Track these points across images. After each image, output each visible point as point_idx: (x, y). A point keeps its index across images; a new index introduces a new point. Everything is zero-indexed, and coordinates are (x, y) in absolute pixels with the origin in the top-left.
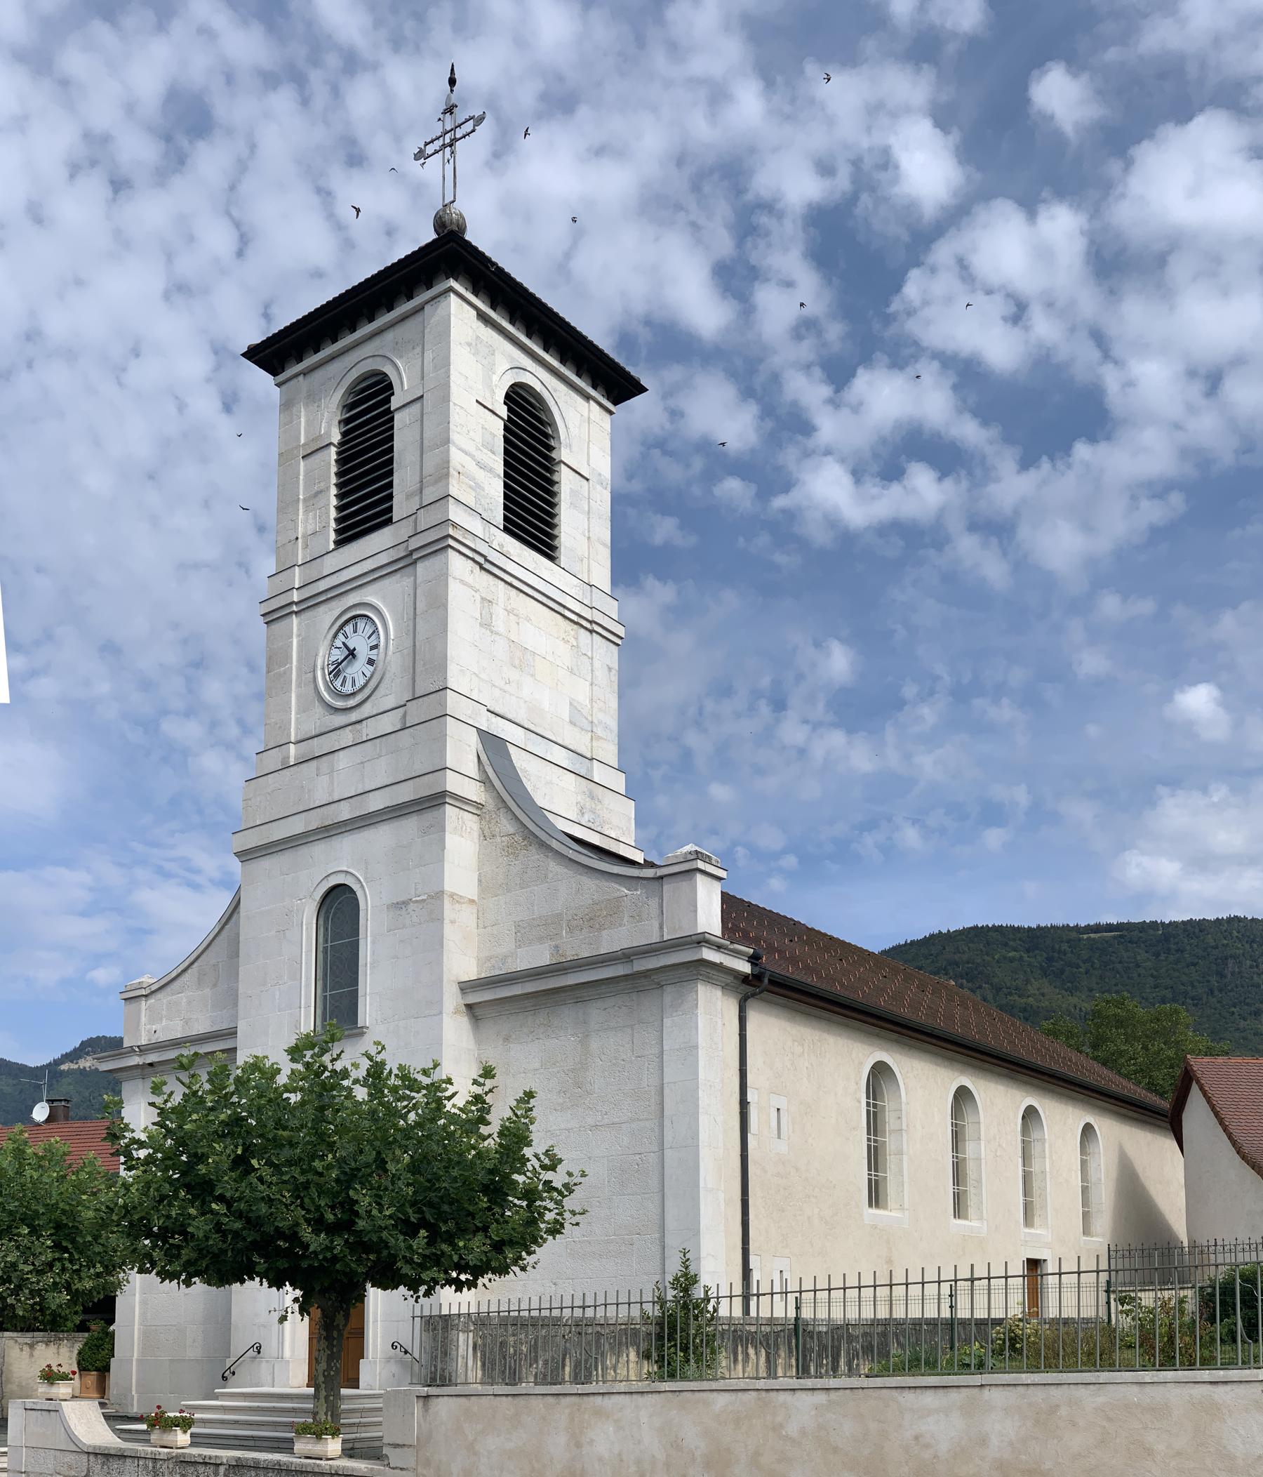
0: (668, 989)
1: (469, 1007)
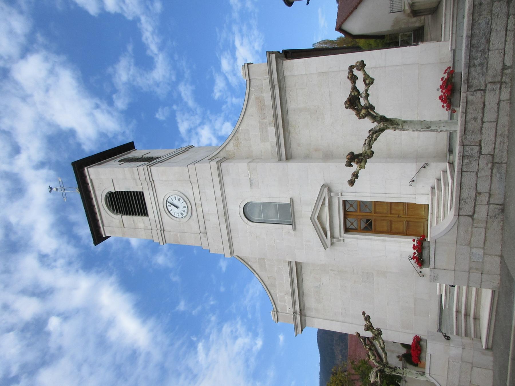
0: (285, 73)
1: (287, 159)
